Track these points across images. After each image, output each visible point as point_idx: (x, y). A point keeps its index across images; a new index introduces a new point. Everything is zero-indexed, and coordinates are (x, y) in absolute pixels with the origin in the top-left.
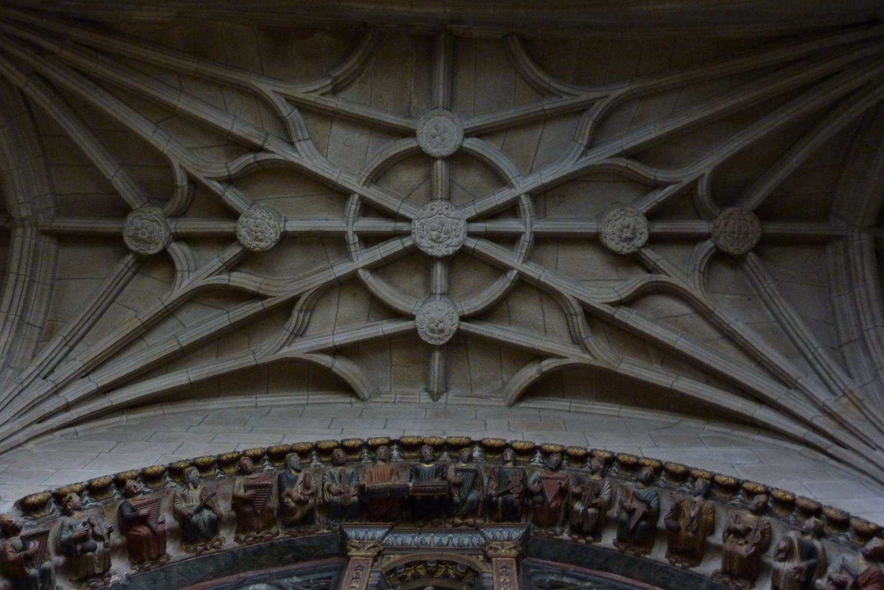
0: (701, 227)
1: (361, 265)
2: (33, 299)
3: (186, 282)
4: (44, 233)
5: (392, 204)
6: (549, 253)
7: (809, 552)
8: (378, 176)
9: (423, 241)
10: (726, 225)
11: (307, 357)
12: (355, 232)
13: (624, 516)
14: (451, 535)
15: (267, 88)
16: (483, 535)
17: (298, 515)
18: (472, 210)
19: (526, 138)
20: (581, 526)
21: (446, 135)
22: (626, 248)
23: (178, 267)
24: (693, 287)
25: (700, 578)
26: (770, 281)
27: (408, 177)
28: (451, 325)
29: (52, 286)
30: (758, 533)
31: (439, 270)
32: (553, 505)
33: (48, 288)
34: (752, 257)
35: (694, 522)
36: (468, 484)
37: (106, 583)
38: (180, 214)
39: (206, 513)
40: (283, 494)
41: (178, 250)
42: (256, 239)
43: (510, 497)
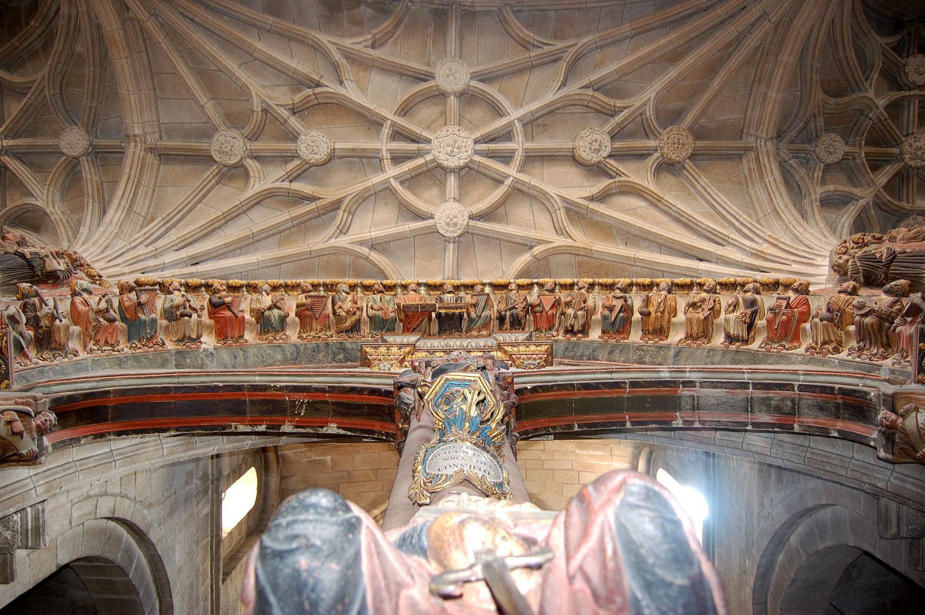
0: (652, 143)
1: (393, 175)
2: (139, 196)
3: (257, 186)
4: (151, 150)
5: (417, 130)
6: (537, 169)
7: (753, 303)
8: (405, 110)
9: (441, 155)
10: (668, 139)
11: (350, 247)
12: (387, 150)
13: (607, 312)
14: (469, 340)
15: (324, 39)
16: (495, 339)
17: (348, 324)
18: (477, 134)
19: (517, 83)
20: (572, 327)
21: (457, 75)
22: (594, 158)
23: (252, 174)
24: (648, 182)
25: (668, 347)
26: (703, 177)
27: (427, 112)
28: (462, 220)
29: (154, 190)
30: (711, 301)
31: (452, 181)
32: (550, 312)
33: (150, 191)
34: (688, 164)
35: (662, 305)
36: (481, 304)
37: (198, 348)
38: (254, 137)
39: (276, 312)
40: (336, 307)
41: (251, 164)
42: (312, 152)
43: (514, 311)
